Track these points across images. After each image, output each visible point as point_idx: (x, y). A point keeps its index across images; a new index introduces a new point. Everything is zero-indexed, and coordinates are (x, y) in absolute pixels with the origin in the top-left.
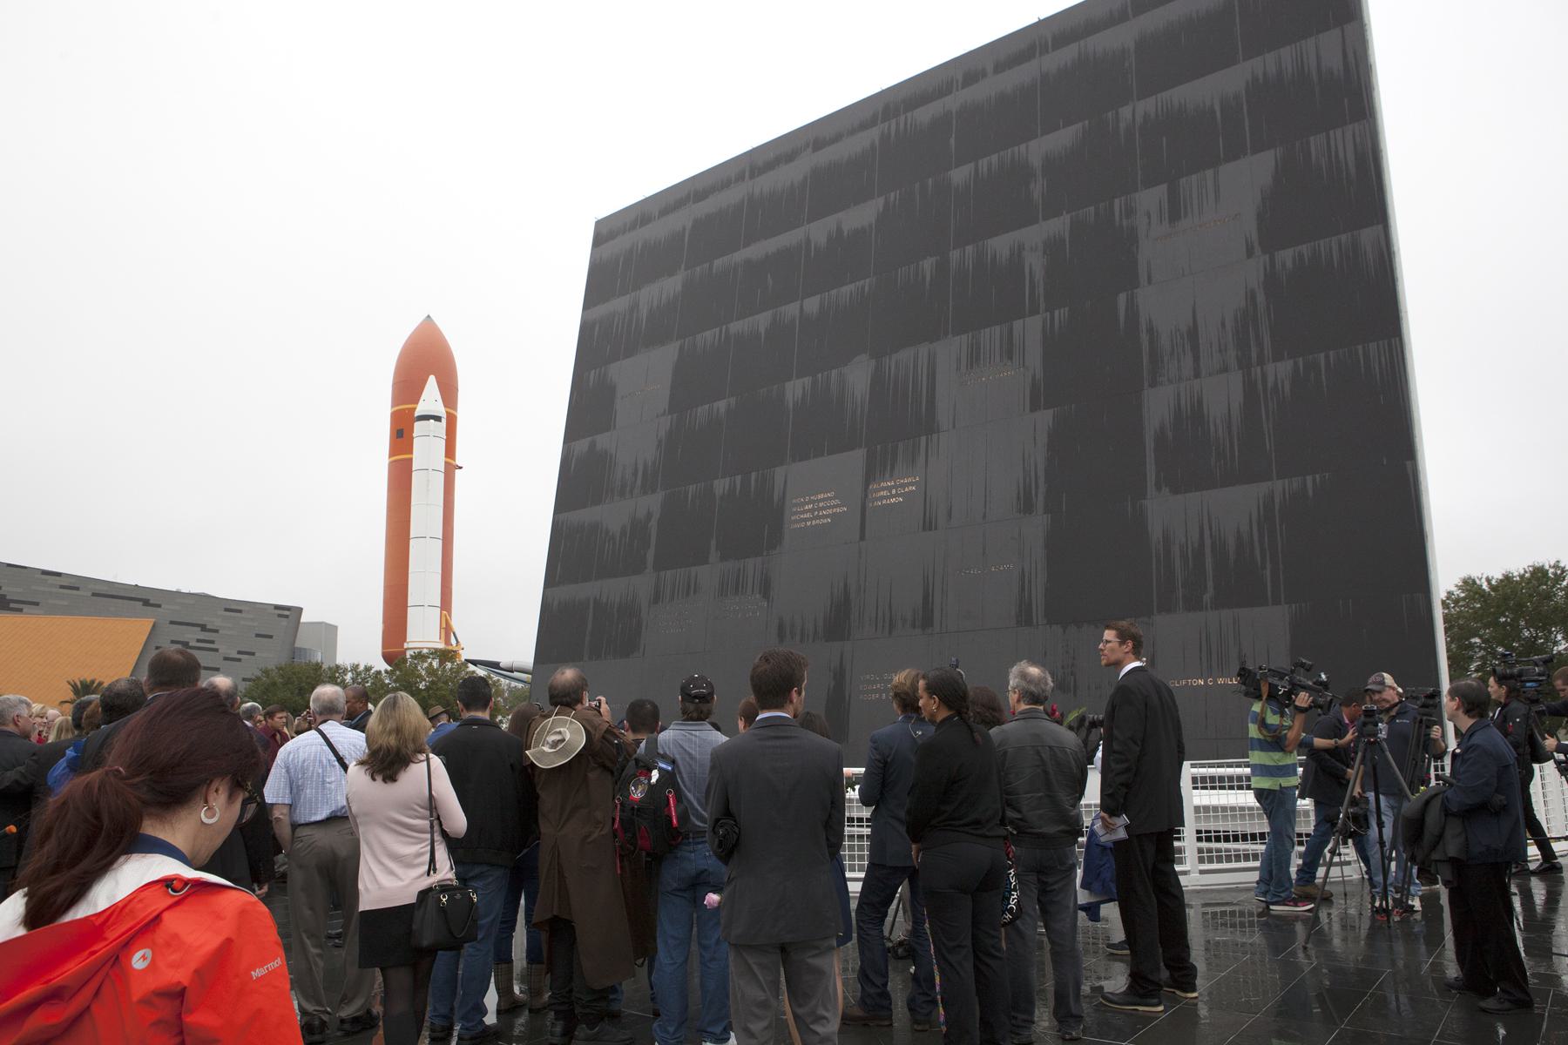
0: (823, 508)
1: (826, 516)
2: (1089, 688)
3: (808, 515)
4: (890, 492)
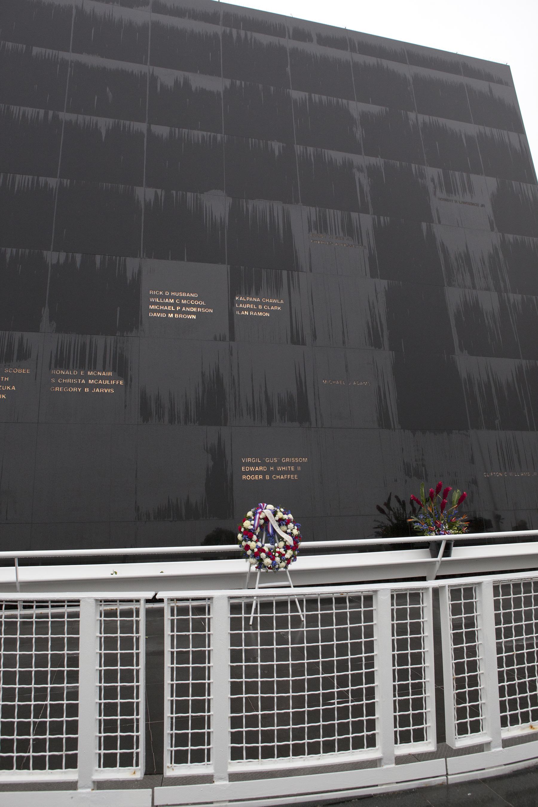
0: (186, 305)
2: (435, 476)
4: (257, 306)
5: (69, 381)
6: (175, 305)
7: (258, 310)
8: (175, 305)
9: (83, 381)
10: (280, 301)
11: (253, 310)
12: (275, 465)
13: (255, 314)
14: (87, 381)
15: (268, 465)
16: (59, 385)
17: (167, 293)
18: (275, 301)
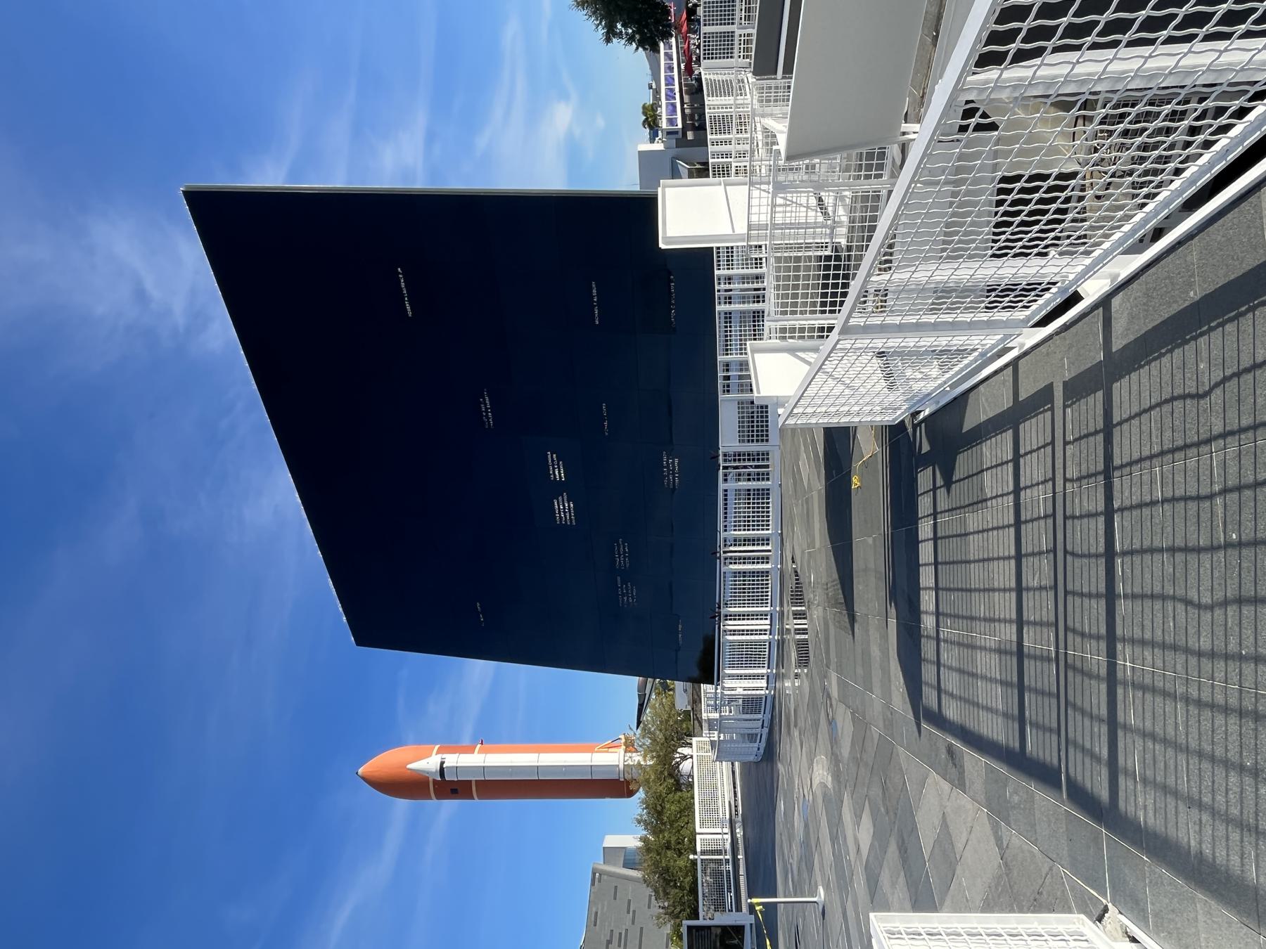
1: (569, 506)
3: (568, 514)
8: (565, 512)
12: (669, 470)
15: (669, 474)
18: (549, 456)
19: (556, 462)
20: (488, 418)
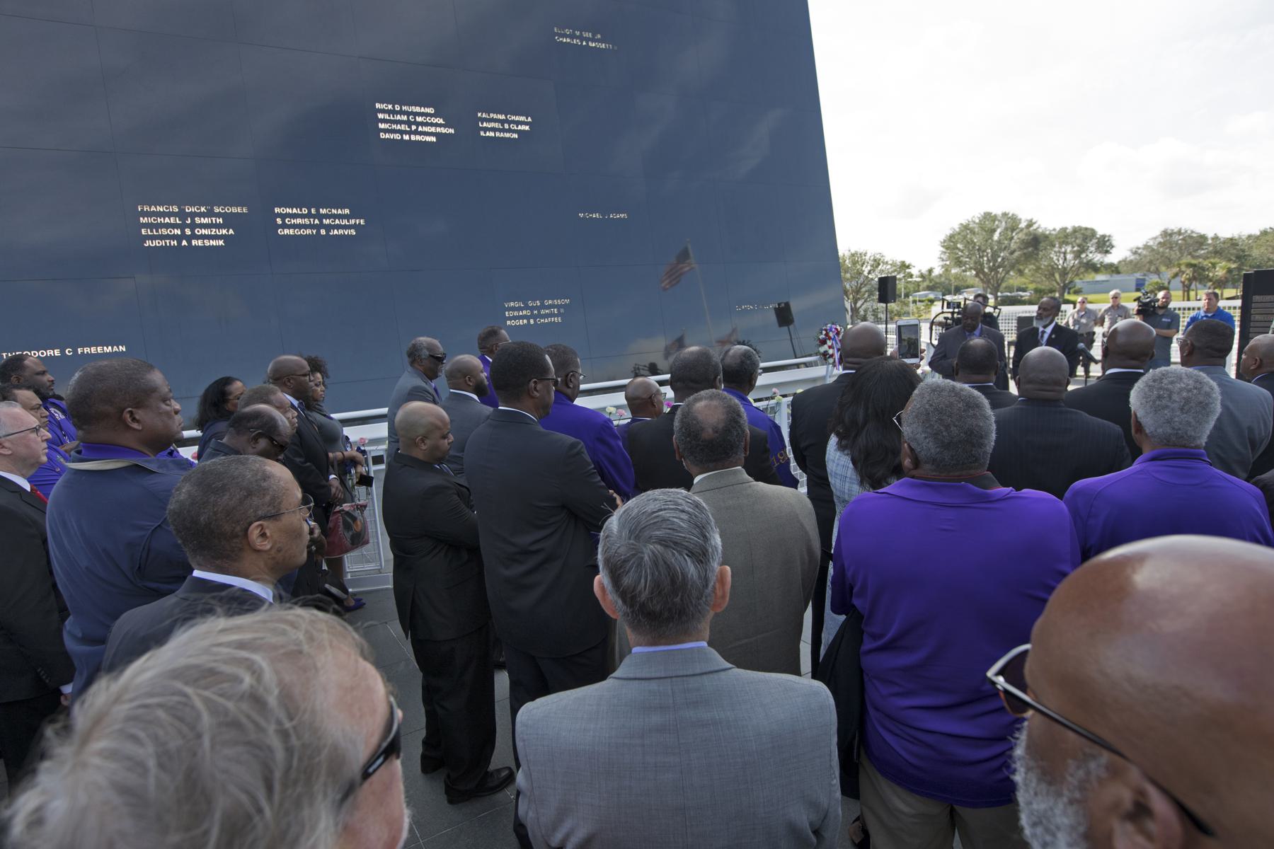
0: (422, 124)
5: (299, 221)
6: (409, 123)
7: (504, 130)
8: (409, 123)
9: (317, 222)
10: (527, 119)
11: (500, 130)
12: (538, 308)
13: (502, 135)
14: (321, 221)
15: (532, 309)
16: (290, 227)
17: (397, 108)
18: (522, 118)
19: (514, 127)
20: (572, 37)
